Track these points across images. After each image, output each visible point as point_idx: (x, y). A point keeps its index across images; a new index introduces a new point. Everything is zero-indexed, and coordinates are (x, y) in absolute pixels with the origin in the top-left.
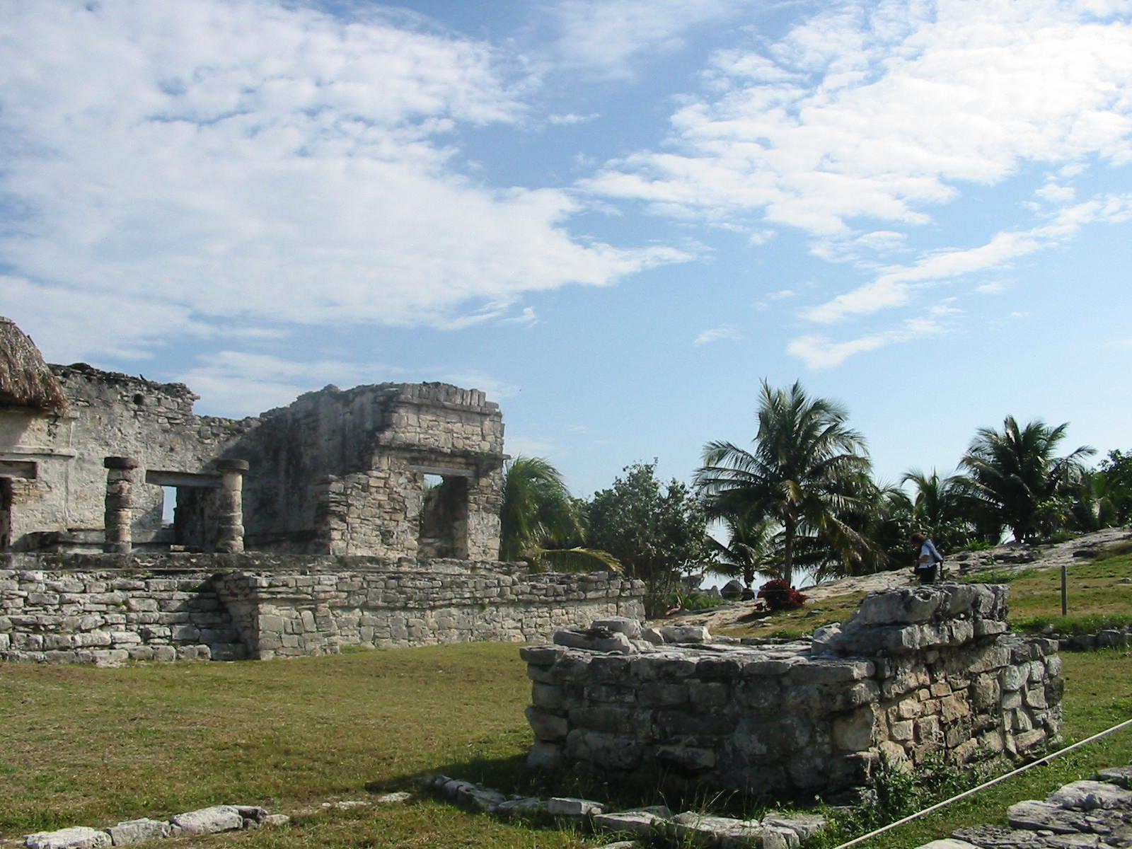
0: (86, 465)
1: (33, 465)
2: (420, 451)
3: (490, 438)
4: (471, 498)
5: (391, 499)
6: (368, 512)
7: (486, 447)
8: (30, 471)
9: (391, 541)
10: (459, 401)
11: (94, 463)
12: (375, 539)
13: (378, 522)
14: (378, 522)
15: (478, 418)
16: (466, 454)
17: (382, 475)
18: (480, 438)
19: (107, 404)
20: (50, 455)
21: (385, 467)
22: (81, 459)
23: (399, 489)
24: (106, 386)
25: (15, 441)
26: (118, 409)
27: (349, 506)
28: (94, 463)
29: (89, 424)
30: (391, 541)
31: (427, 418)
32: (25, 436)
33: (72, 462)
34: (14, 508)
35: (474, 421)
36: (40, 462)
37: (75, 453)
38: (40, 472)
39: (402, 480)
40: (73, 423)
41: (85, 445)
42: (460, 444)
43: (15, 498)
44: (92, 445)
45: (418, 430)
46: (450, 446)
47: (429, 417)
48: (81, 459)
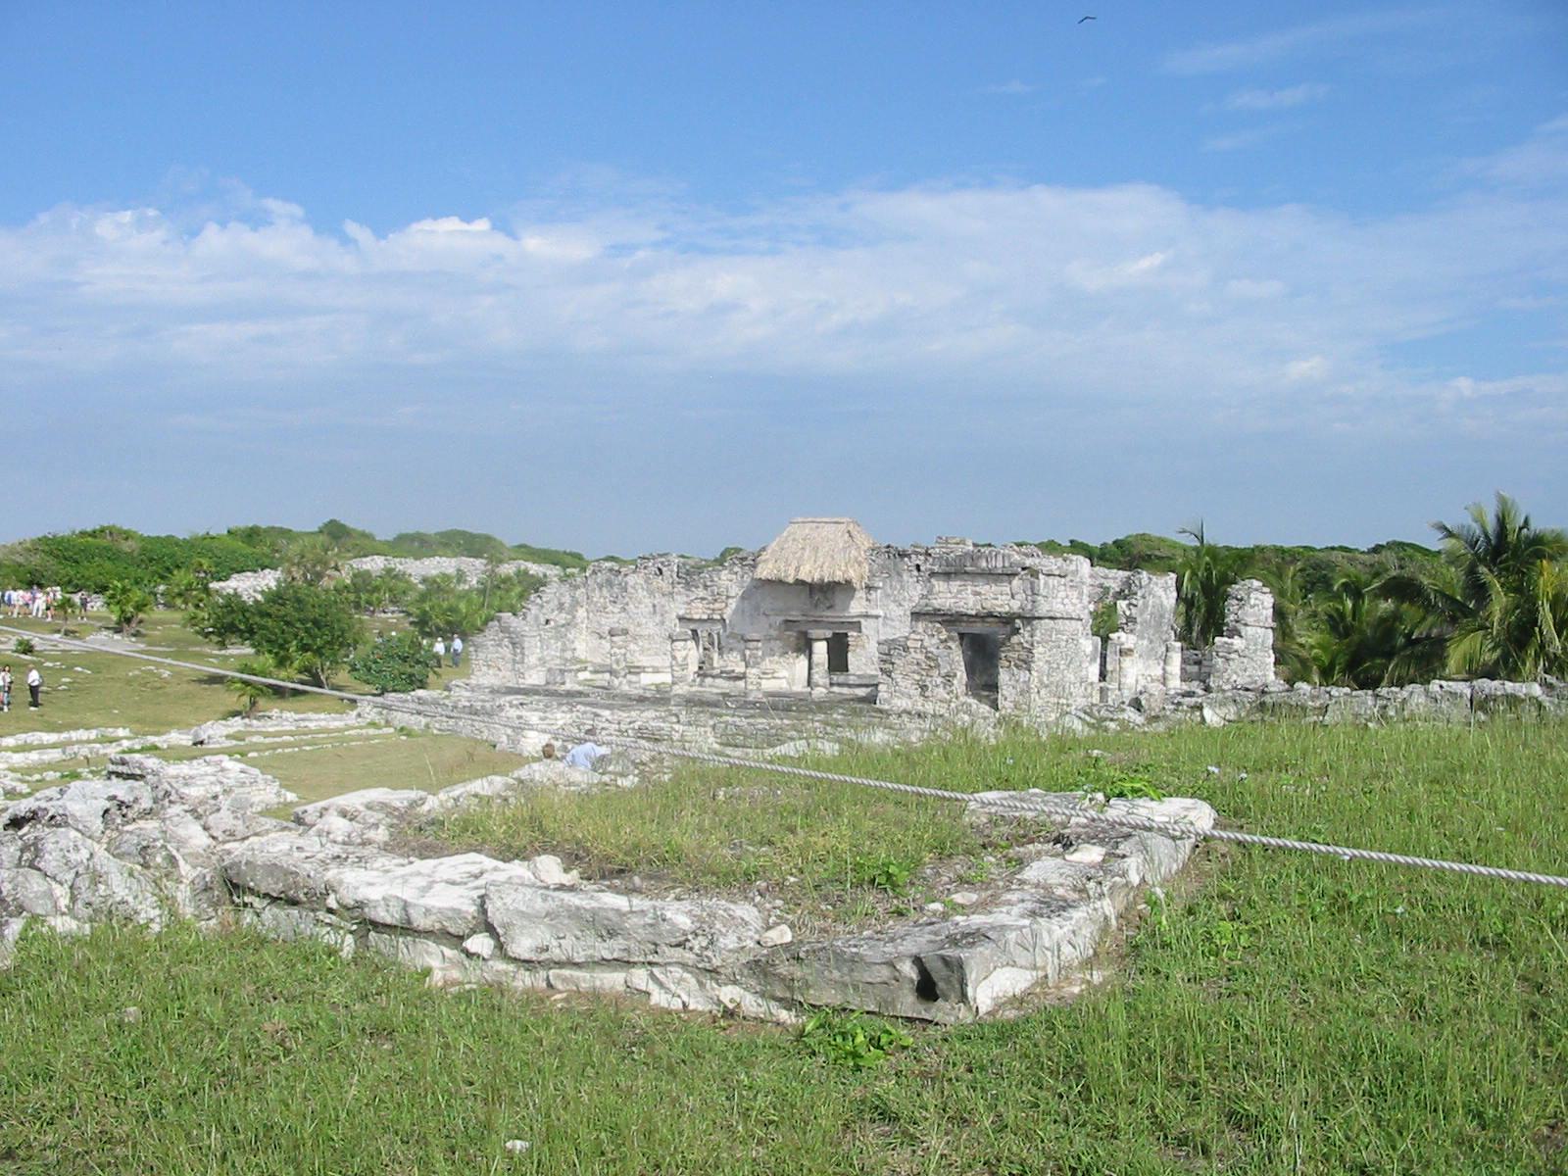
0: (889, 622)
1: (859, 622)
2: (951, 615)
3: (1021, 596)
4: (1003, 655)
5: (928, 658)
6: (908, 668)
7: (1015, 606)
8: (857, 626)
9: (927, 694)
10: (984, 564)
11: (892, 620)
12: (915, 692)
13: (917, 677)
14: (917, 677)
15: (1006, 578)
16: (990, 615)
17: (918, 637)
18: (1009, 597)
19: (899, 574)
20: (867, 616)
21: (921, 630)
22: (885, 617)
23: (932, 649)
24: (898, 559)
25: (846, 608)
26: (905, 577)
27: (893, 664)
28: (892, 620)
29: (889, 591)
30: (927, 694)
31: (955, 585)
32: (853, 604)
33: (880, 619)
34: (850, 655)
35: (1002, 581)
36: (862, 620)
37: (881, 613)
38: (863, 630)
39: (935, 641)
40: (879, 591)
41: (887, 606)
42: (988, 605)
43: (850, 648)
44: (893, 606)
45: (949, 595)
46: (979, 607)
47: (958, 583)
48: (885, 617)
